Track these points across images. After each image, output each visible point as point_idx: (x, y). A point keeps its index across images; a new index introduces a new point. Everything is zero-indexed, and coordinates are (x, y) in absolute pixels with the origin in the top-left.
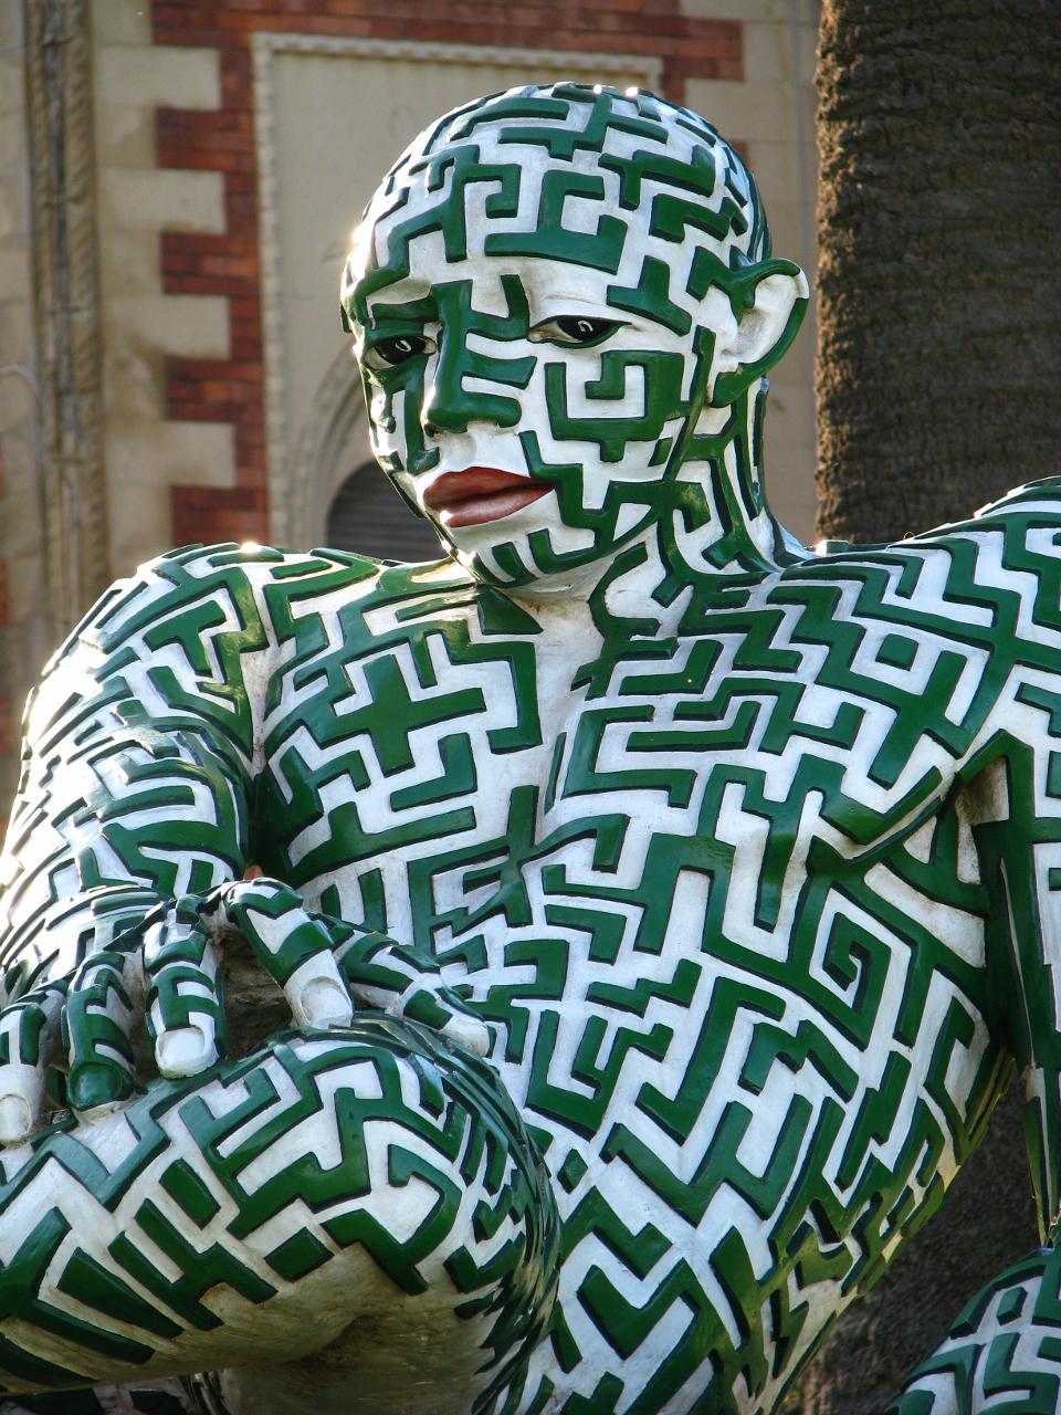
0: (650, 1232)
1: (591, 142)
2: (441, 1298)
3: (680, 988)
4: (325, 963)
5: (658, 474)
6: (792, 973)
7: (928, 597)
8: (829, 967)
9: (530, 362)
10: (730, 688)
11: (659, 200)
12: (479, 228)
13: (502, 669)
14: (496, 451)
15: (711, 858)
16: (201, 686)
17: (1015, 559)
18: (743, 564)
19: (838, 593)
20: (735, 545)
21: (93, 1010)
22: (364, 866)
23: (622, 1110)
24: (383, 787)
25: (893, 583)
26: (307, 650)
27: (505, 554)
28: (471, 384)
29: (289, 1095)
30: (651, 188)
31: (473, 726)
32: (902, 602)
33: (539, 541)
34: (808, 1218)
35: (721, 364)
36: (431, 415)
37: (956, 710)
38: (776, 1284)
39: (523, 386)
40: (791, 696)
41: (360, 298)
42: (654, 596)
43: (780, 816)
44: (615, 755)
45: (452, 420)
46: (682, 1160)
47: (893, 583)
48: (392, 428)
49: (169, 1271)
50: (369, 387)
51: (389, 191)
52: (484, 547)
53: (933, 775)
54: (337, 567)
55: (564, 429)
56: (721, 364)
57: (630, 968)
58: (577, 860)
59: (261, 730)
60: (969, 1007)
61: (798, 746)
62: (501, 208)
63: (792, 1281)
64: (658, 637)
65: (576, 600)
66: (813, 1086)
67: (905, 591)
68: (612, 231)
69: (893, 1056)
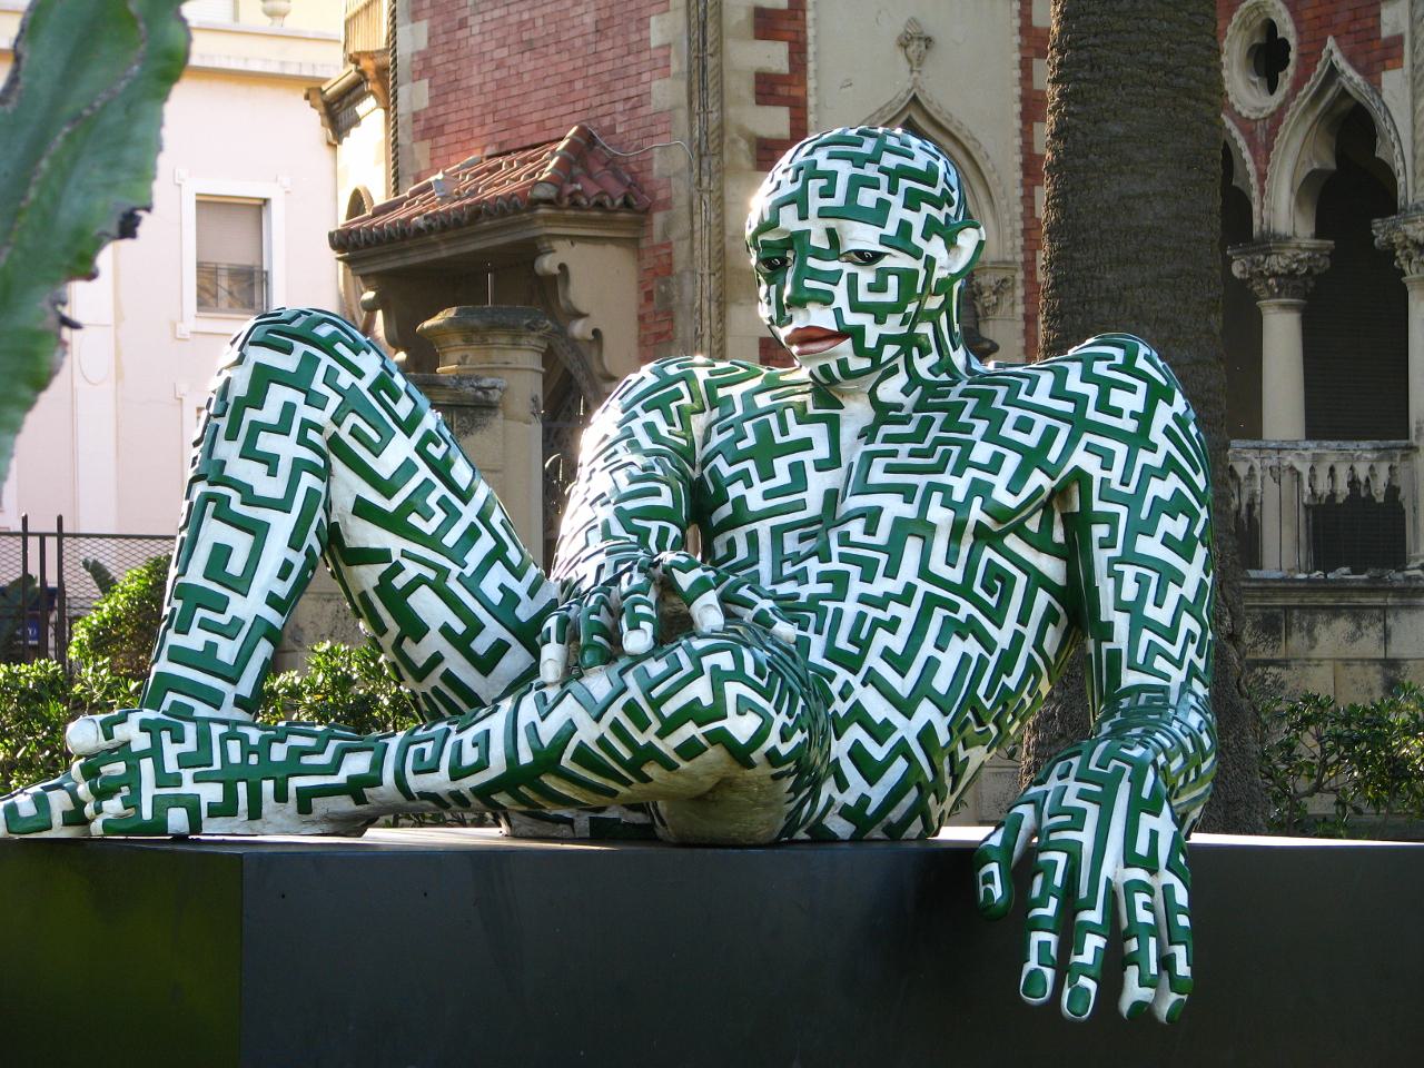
0: (886, 722)
1: (874, 159)
2: (763, 770)
3: (906, 597)
4: (711, 597)
5: (905, 330)
6: (964, 590)
7: (1041, 397)
8: (983, 586)
9: (840, 272)
10: (938, 441)
11: (908, 191)
12: (815, 203)
13: (823, 427)
14: (821, 317)
15: (924, 529)
16: (669, 432)
17: (1087, 377)
18: (949, 375)
19: (995, 393)
20: (945, 365)
21: (593, 617)
22: (749, 528)
23: (873, 660)
24: (760, 486)
25: (1024, 388)
26: (726, 413)
27: (825, 370)
28: (808, 283)
29: (688, 667)
30: (904, 184)
31: (807, 457)
32: (1028, 399)
33: (842, 363)
34: (969, 715)
35: (938, 274)
36: (788, 299)
37: (1053, 456)
38: (952, 747)
39: (836, 284)
40: (968, 446)
41: (754, 237)
42: (902, 391)
43: (960, 509)
44: (877, 475)
45: (799, 302)
46: (903, 686)
47: (1024, 388)
48: (769, 303)
49: (626, 754)
50: (759, 281)
51: (772, 180)
52: (815, 366)
53: (1040, 489)
54: (742, 371)
55: (856, 307)
56: (938, 274)
57: (881, 586)
58: (856, 529)
59: (700, 455)
60: (1057, 606)
61: (971, 473)
62: (827, 193)
63: (960, 746)
64: (903, 413)
65: (862, 392)
66: (973, 647)
67: (1030, 392)
68: (883, 206)
69: (1016, 631)
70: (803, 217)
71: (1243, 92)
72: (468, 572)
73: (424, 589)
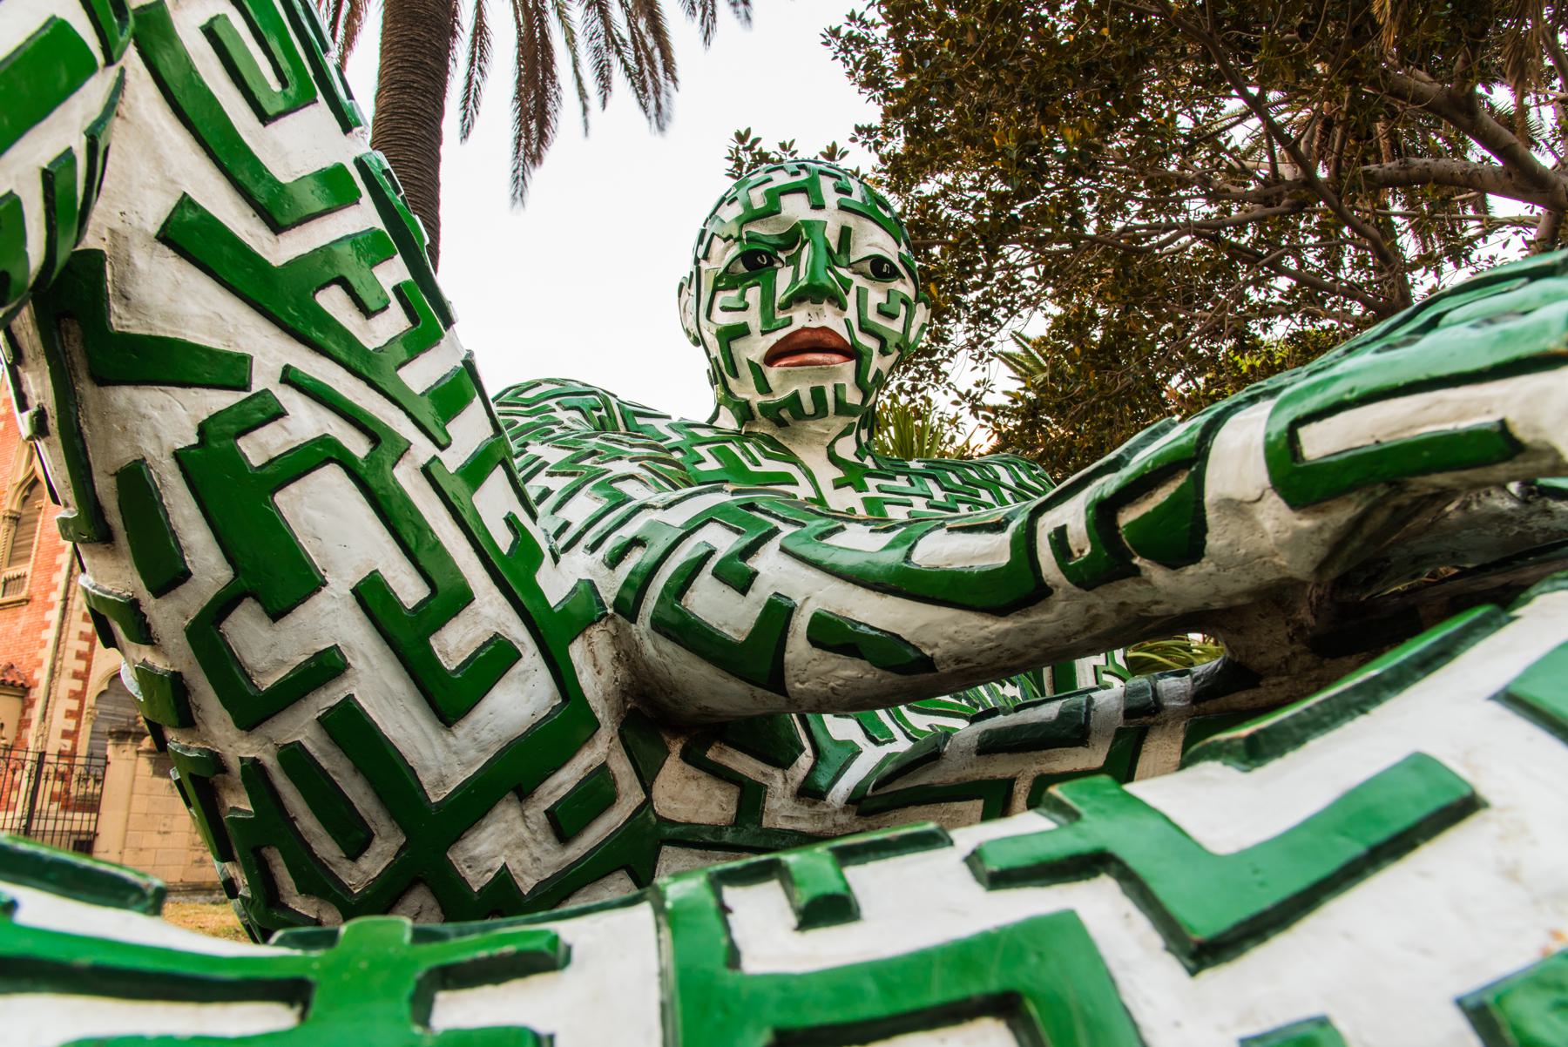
12: (831, 198)
55: (866, 329)
70: (818, 206)
72: (453, 460)
73: (332, 475)
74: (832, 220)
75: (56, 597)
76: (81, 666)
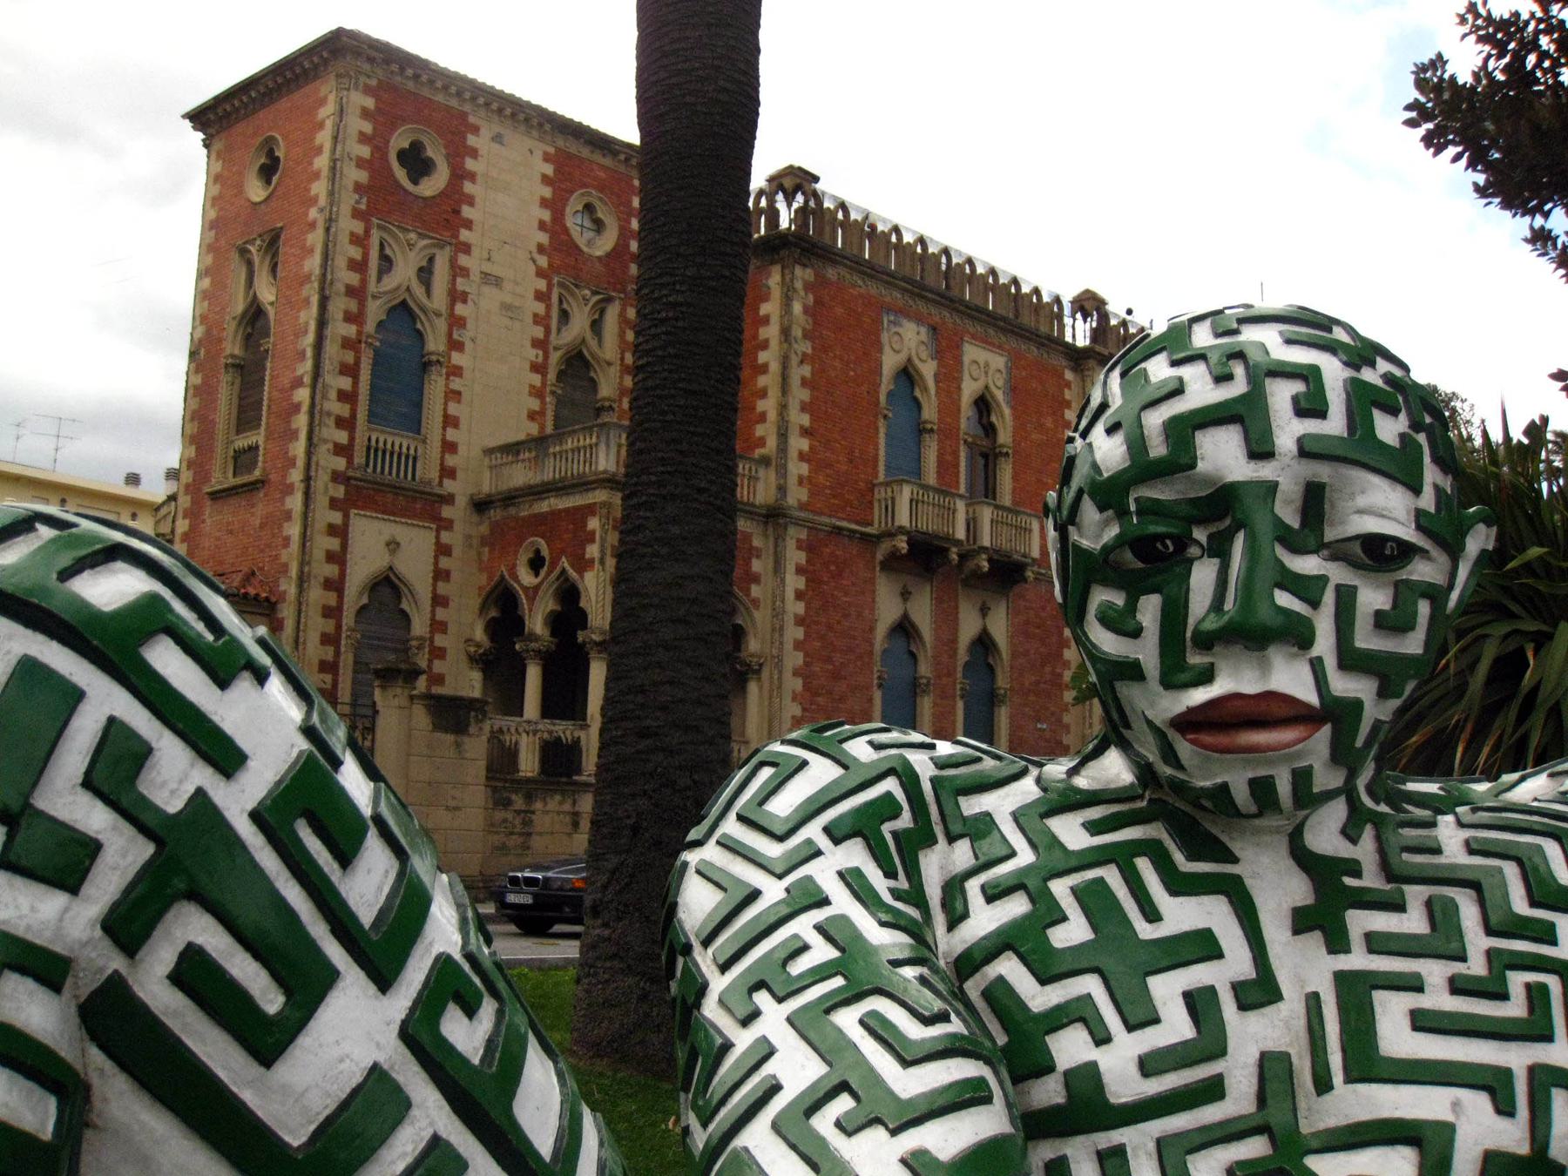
9: (1322, 580)
12: (1288, 431)
33: (1302, 778)
55: (1350, 660)
62: (1311, 406)
70: (1260, 450)
71: (526, 577)
74: (1285, 472)
75: (296, 476)
76: (332, 570)
